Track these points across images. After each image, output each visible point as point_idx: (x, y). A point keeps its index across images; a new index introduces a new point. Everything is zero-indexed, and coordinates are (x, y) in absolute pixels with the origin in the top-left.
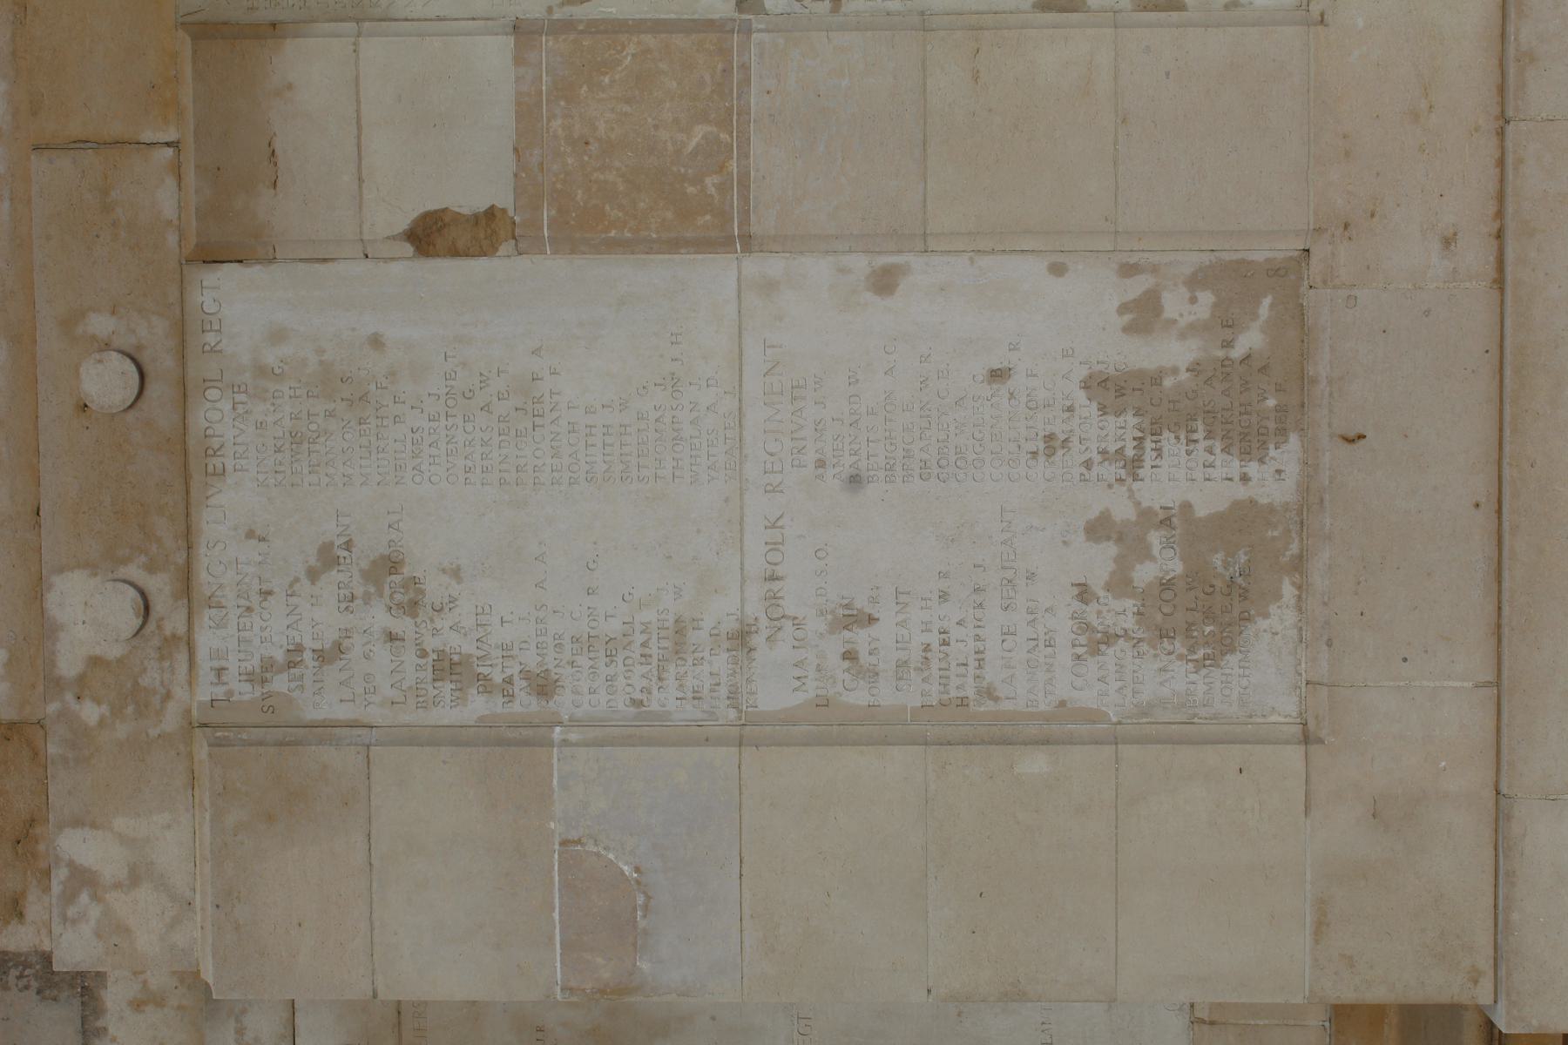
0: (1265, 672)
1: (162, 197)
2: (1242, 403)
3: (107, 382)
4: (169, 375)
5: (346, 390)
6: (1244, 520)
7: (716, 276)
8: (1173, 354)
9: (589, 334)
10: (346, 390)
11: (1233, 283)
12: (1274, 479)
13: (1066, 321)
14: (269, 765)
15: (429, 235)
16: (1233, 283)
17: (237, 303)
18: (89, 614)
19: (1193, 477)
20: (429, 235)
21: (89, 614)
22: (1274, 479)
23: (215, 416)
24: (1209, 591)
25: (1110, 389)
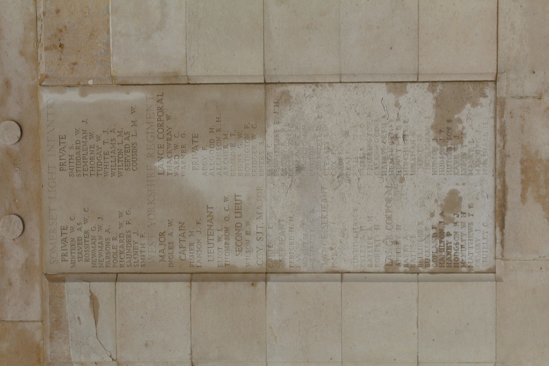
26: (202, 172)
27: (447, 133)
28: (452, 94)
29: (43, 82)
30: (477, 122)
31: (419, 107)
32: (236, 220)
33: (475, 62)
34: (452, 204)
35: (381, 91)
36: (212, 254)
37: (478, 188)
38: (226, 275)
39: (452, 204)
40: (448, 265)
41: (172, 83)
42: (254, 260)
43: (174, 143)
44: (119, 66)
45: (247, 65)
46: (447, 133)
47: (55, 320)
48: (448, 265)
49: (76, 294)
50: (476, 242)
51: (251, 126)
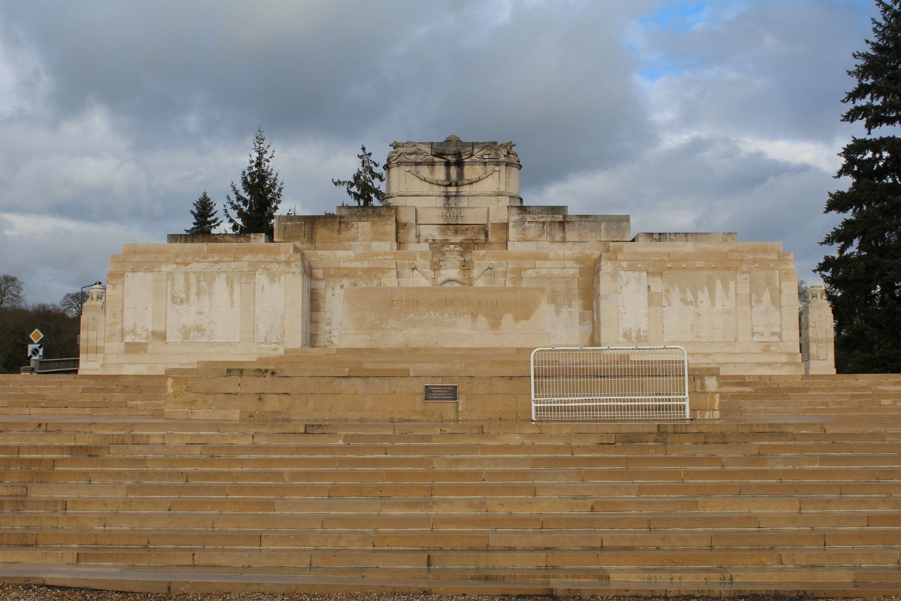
0: (622, 339)
1: (651, 270)
2: (639, 338)
3: (639, 266)
4: (639, 270)
5: (639, 281)
6: (631, 338)
7: (646, 305)
8: (642, 333)
9: (643, 296)
10: (639, 281)
11: (646, 337)
12: (634, 340)
13: (644, 327)
14: (614, 276)
15: (649, 286)
16: (646, 337)
17: (645, 274)
18: (624, 264)
19: (634, 335)
20: (649, 286)
21: (624, 264)
22: (634, 340)
23: (637, 273)
24: (627, 336)
25: (639, 329)
26: (766, 296)
27: (773, 334)
28: (779, 335)
29: (780, 272)
30: (775, 338)
31: (777, 330)
32: (759, 301)
33: (784, 338)
34: (762, 335)
35: (779, 323)
36: (754, 297)
37: (765, 339)
38: (751, 300)
39: (762, 335)
40: (753, 334)
41: (780, 292)
42: (753, 304)
43: (771, 292)
44: (783, 283)
45: (783, 303)
46: (773, 334)
47: (743, 272)
48: (753, 334)
49: (747, 276)
50: (757, 338)
51: (773, 303)
